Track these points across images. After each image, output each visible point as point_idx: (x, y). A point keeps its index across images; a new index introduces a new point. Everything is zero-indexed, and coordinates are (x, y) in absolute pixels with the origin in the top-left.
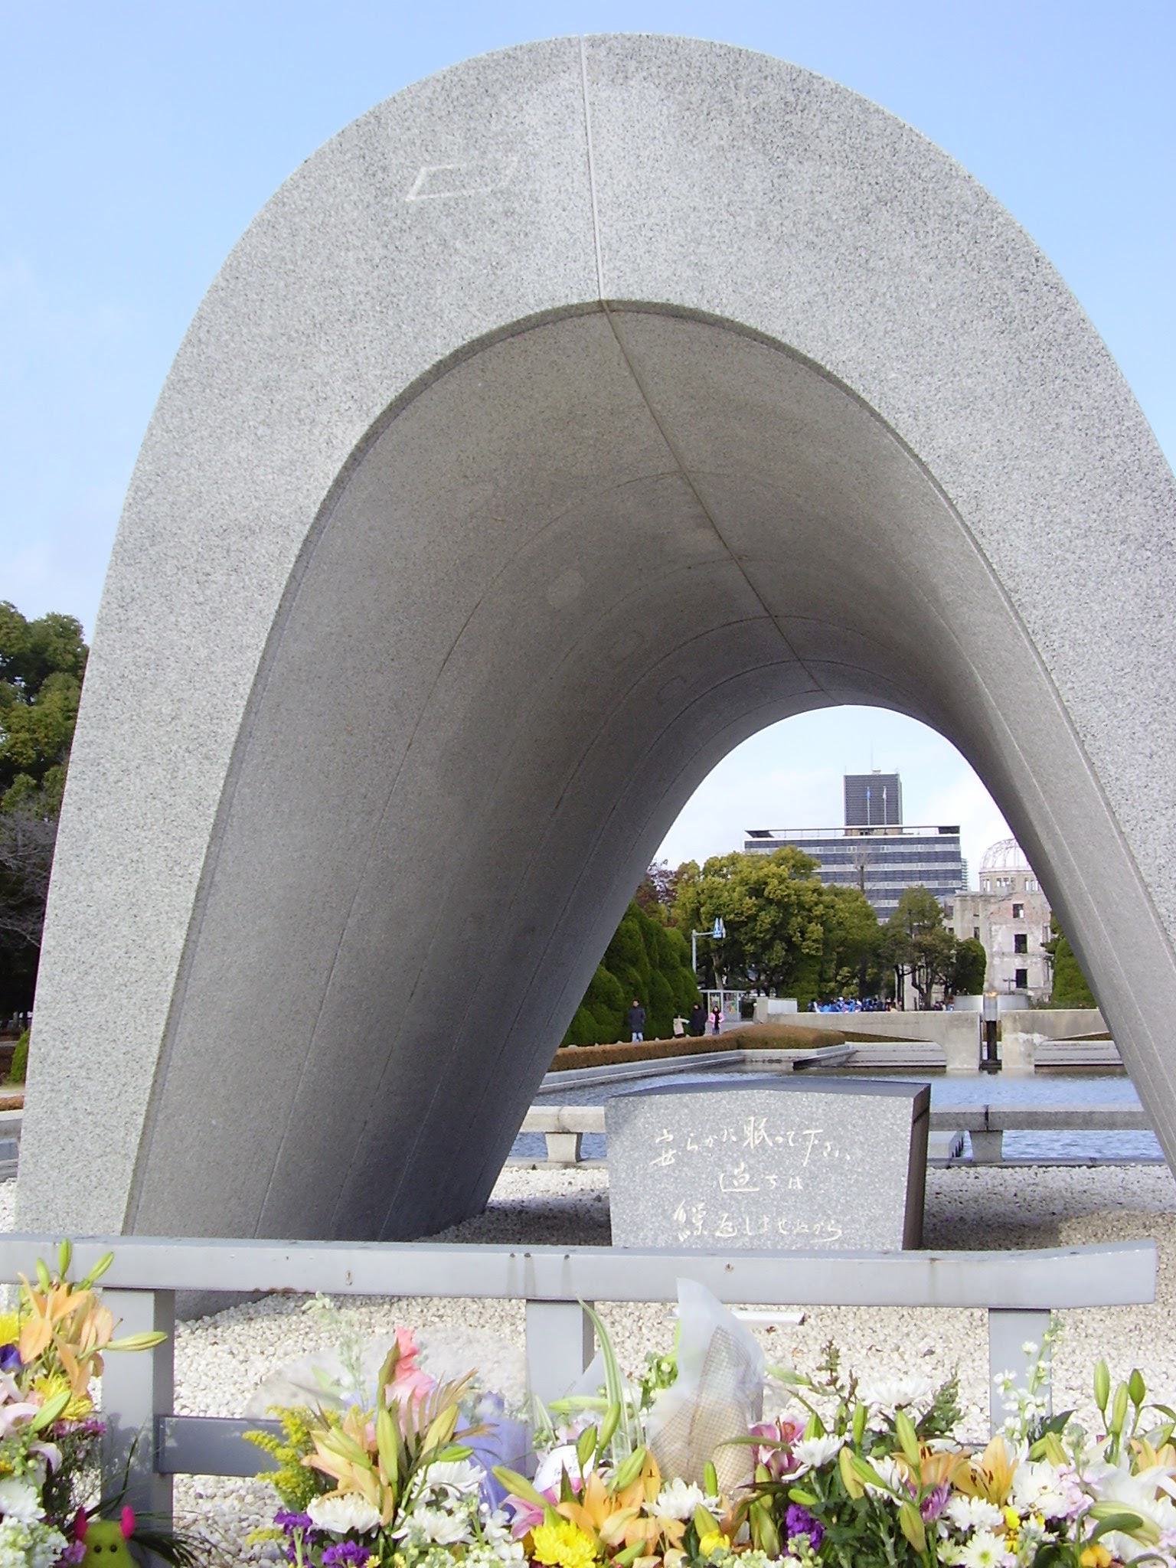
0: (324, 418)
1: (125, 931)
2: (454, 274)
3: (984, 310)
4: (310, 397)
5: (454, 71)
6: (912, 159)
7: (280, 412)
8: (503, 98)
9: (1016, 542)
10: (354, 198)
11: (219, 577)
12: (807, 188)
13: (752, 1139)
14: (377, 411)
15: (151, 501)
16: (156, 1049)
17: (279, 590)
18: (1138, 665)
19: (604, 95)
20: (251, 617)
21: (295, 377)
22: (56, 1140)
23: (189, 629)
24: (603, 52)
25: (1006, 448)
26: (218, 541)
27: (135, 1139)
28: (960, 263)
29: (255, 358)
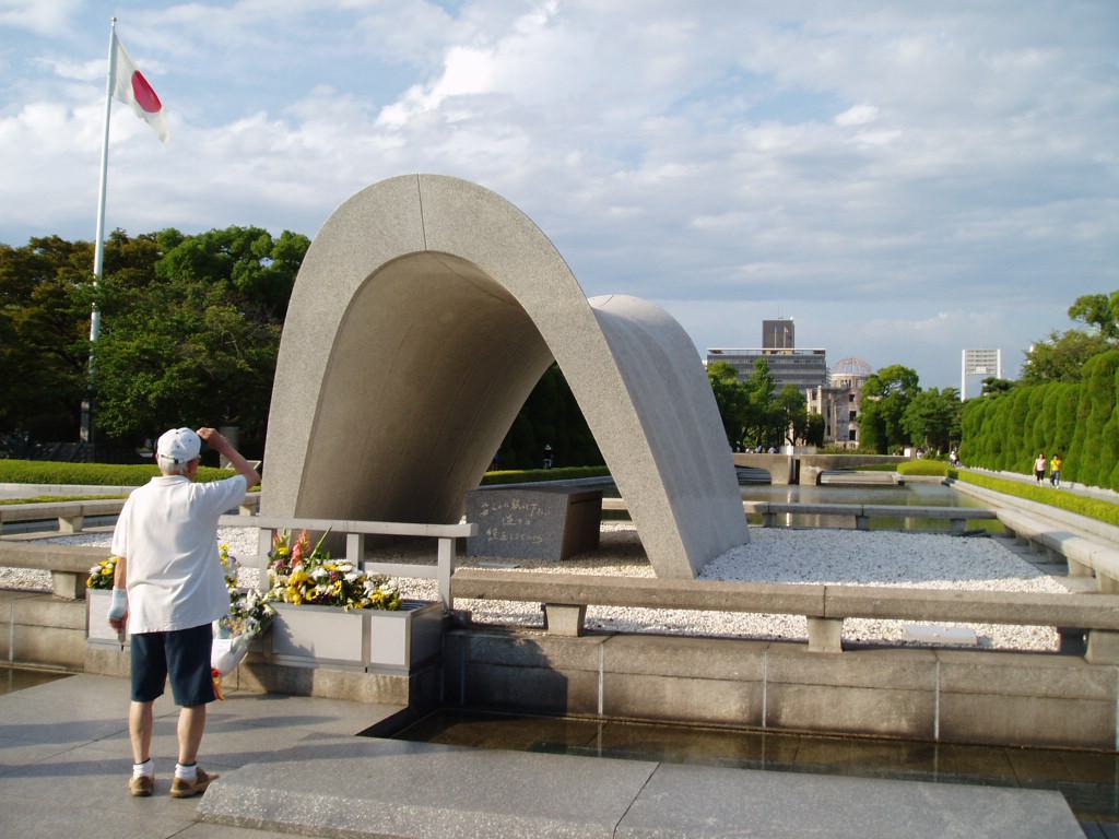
11: (318, 327)
13: (514, 507)
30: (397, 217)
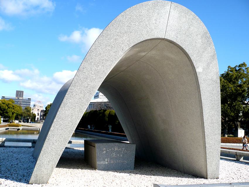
1: (69, 119)
2: (146, 30)
4: (122, 42)
7: (116, 44)
9: (202, 79)
12: (192, 30)
15: (93, 53)
18: (210, 96)
20: (104, 73)
29: (115, 35)
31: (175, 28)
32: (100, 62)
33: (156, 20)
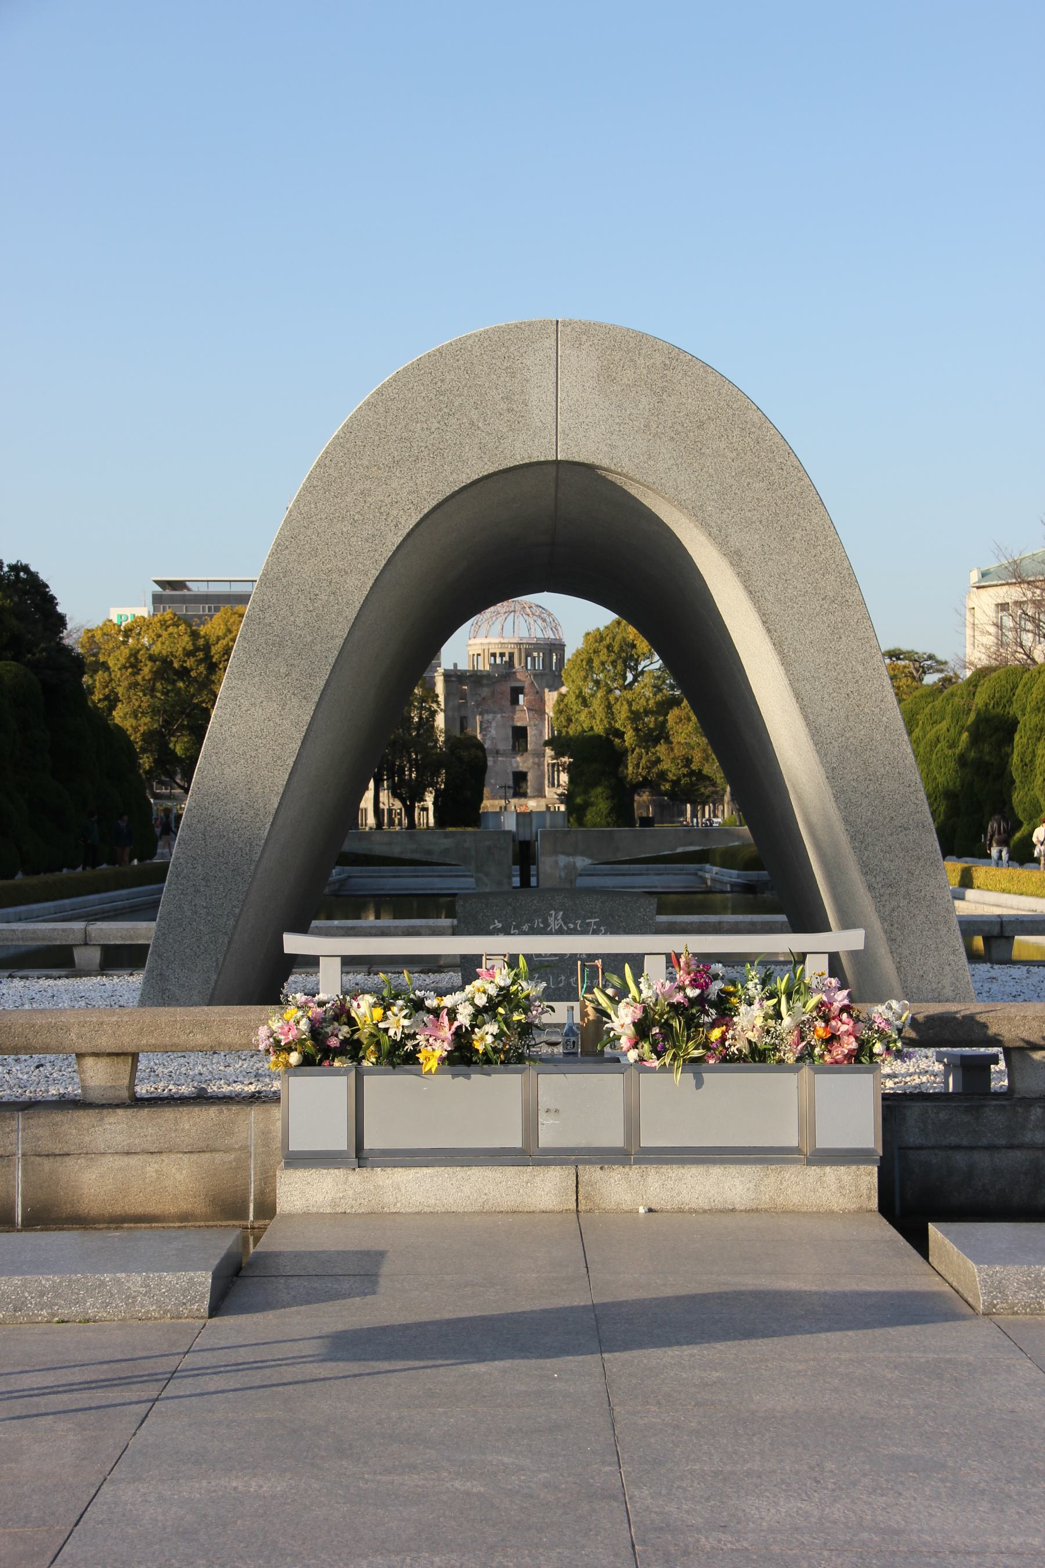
0: (395, 512)
1: (242, 797)
2: (477, 440)
3: (760, 478)
5: (486, 332)
6: (728, 398)
8: (512, 349)
10: (423, 395)
11: (323, 597)
12: (672, 409)
14: (426, 511)
15: (286, 552)
16: (252, 867)
17: (358, 606)
19: (567, 352)
20: (341, 620)
21: (380, 489)
22: (180, 925)
23: (302, 625)
24: (569, 329)
25: (766, 548)
26: (325, 577)
27: (232, 922)
28: (749, 453)
30: (506, 398)
31: (594, 415)
32: (319, 580)
33: (506, 398)
